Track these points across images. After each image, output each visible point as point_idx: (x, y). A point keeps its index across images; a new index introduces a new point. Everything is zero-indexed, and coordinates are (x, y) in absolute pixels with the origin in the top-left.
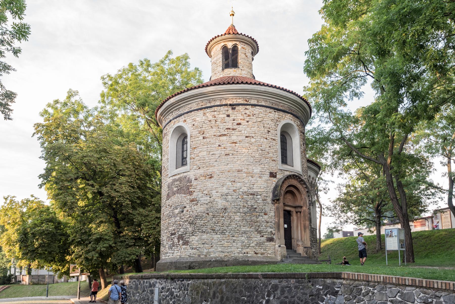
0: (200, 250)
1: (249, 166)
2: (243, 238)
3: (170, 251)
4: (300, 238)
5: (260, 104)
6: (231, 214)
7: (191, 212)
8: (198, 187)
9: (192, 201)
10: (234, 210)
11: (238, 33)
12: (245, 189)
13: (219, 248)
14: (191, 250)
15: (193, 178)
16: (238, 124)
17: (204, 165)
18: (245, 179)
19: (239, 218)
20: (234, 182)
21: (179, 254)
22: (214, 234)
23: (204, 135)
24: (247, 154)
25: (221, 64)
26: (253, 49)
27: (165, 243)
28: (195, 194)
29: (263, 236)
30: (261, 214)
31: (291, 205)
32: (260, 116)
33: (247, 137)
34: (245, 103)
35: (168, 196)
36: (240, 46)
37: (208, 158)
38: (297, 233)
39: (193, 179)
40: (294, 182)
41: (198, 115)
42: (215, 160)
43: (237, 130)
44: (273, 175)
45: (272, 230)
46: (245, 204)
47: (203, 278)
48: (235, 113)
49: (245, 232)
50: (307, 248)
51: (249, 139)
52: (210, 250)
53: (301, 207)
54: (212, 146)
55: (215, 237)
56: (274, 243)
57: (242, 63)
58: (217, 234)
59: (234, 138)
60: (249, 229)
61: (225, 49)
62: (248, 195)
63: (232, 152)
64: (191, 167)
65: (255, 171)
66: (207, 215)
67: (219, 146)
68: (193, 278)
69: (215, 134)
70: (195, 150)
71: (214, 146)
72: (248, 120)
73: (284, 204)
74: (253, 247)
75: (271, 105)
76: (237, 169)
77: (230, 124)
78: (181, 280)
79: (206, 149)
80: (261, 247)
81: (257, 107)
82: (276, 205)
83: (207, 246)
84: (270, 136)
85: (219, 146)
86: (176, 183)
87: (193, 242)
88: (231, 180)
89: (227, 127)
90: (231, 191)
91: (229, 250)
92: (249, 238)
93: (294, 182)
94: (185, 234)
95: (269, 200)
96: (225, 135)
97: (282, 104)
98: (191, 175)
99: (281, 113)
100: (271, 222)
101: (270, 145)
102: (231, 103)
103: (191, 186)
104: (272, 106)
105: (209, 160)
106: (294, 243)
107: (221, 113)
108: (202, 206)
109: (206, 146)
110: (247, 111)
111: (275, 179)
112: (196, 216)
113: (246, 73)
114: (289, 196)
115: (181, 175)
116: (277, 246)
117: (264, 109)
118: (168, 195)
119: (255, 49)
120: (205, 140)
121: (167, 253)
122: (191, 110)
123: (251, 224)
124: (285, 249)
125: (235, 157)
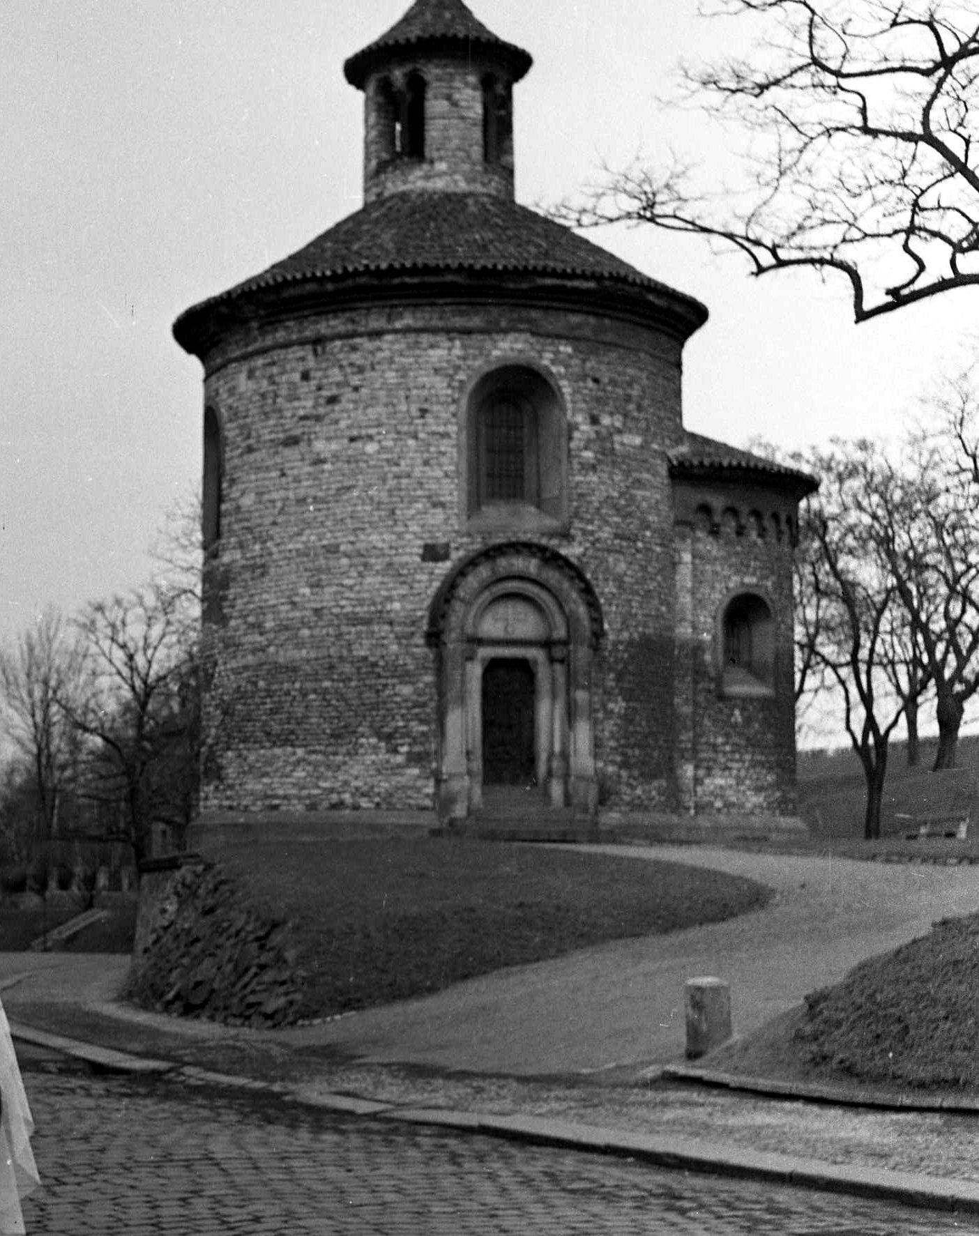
1: (359, 532)
20: (318, 586)
28: (233, 623)
30: (389, 681)
33: (352, 439)
42: (271, 519)
43: (327, 421)
44: (433, 553)
46: (345, 653)
48: (324, 365)
51: (359, 445)
63: (312, 492)
69: (273, 436)
79: (252, 485)
81: (389, 337)
89: (301, 412)
101: (426, 455)
110: (356, 357)
117: (411, 338)
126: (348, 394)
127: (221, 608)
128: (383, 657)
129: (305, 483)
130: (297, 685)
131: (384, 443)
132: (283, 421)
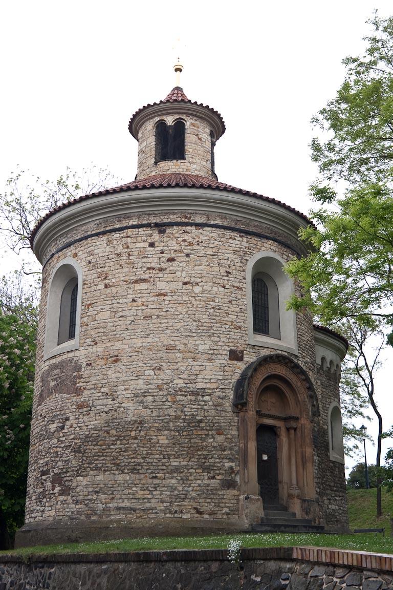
0: (91, 505)
1: (189, 338)
2: (174, 481)
3: (38, 508)
4: (294, 481)
5: (212, 222)
6: (152, 433)
7: (78, 429)
8: (92, 379)
9: (80, 406)
10: (157, 425)
11: (190, 101)
12: (180, 383)
13: (126, 501)
14: (74, 505)
15: (83, 362)
16: (168, 260)
17: (104, 338)
18: (179, 364)
19: (166, 442)
20: (159, 369)
21: (52, 513)
22: (117, 472)
23: (107, 281)
24: (187, 316)
25: (154, 152)
26: (214, 127)
27: (31, 491)
28: (86, 393)
29: (213, 478)
30: (210, 433)
31: (277, 414)
32: (211, 245)
33: (185, 284)
34: (184, 220)
35: (42, 398)
36: (189, 122)
37: (112, 324)
38: (287, 472)
39: (84, 365)
40: (280, 370)
41: (97, 243)
42: (125, 327)
43: (167, 271)
44: (235, 356)
45: (233, 464)
46: (180, 413)
47: (74, 563)
49: (177, 470)
50: (308, 501)
51: (189, 286)
52: (108, 505)
53: (297, 419)
54: (121, 301)
55: (120, 478)
56: (236, 492)
57: (191, 150)
58: (123, 472)
59: (162, 286)
60: (185, 463)
61: (161, 126)
62: (186, 396)
63: (156, 312)
64: (83, 341)
65: (200, 348)
66: (106, 434)
67: (134, 300)
68: (58, 563)
69: (127, 278)
70: (91, 309)
71: (125, 301)
72: (189, 252)
73: (257, 412)
74: (194, 498)
75: (233, 225)
76: (166, 343)
77: (156, 260)
78: (40, 565)
79: (109, 307)
80: (209, 500)
82: (241, 414)
83: (103, 496)
84: (232, 281)
85: (134, 300)
86: (54, 372)
87: (78, 490)
88: (155, 365)
89: (149, 265)
90: (153, 386)
91: (148, 505)
92: (184, 480)
93: (280, 370)
94: (66, 472)
95: (228, 405)
96: (144, 280)
97: (255, 223)
98: (81, 356)
99: (254, 240)
100: (231, 449)
102: (158, 221)
103: (80, 377)
104: (234, 226)
105: (114, 328)
106: (284, 491)
107: (139, 239)
108: (97, 417)
109: (110, 302)
110: (186, 236)
111: (240, 364)
112: (87, 437)
113: (198, 168)
114: (271, 400)
115: (64, 357)
116: (242, 497)
118: (41, 395)
119: (217, 126)
120: (108, 290)
121: (33, 512)
122: (86, 234)
123: (191, 451)
124: (260, 504)
125: (162, 321)
126: (181, 258)
127: (75, 384)
128: (205, 417)
129: (149, 307)
130: (142, 433)
131: (204, 288)
132: (134, 270)
